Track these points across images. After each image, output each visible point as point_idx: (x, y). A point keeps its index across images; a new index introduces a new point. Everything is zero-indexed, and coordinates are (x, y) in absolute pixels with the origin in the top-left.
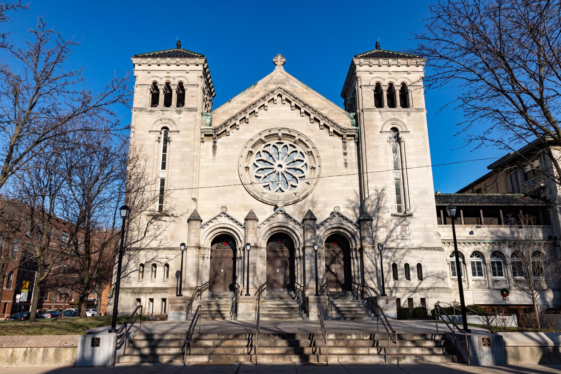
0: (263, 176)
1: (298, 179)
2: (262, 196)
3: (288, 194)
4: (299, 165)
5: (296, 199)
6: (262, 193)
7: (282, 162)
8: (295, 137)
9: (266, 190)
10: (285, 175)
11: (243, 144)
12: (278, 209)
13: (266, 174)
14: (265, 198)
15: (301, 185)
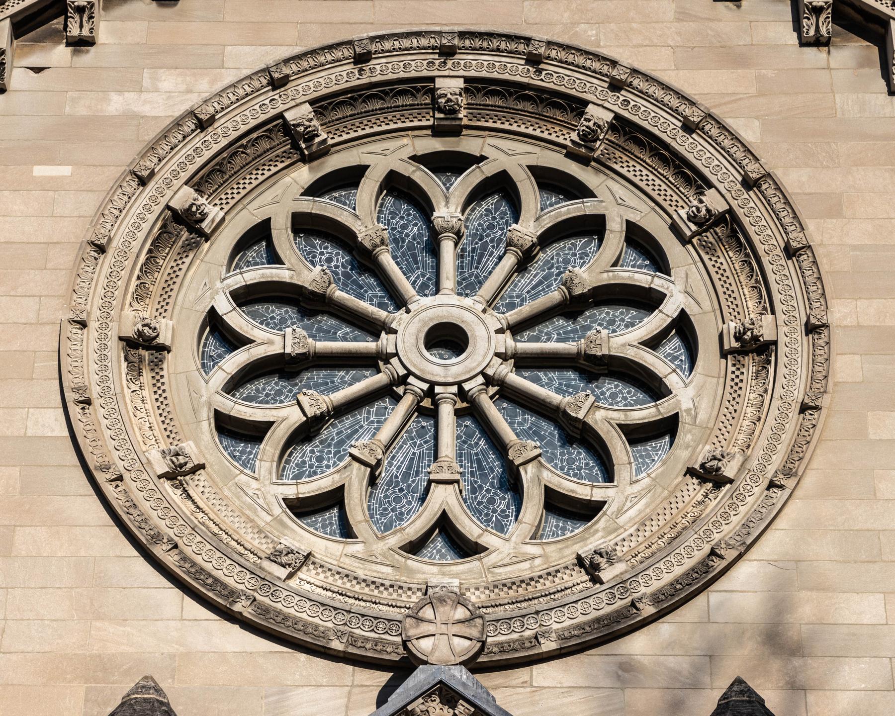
0: (287, 416)
1: (618, 446)
2: (267, 583)
3: (523, 570)
4: (623, 336)
5: (601, 605)
6: (275, 557)
7: (462, 317)
8: (577, 106)
9: (302, 537)
10: (495, 413)
11: (123, 155)
12: (419, 678)
13: (316, 401)
14: (300, 599)
15: (638, 497)
